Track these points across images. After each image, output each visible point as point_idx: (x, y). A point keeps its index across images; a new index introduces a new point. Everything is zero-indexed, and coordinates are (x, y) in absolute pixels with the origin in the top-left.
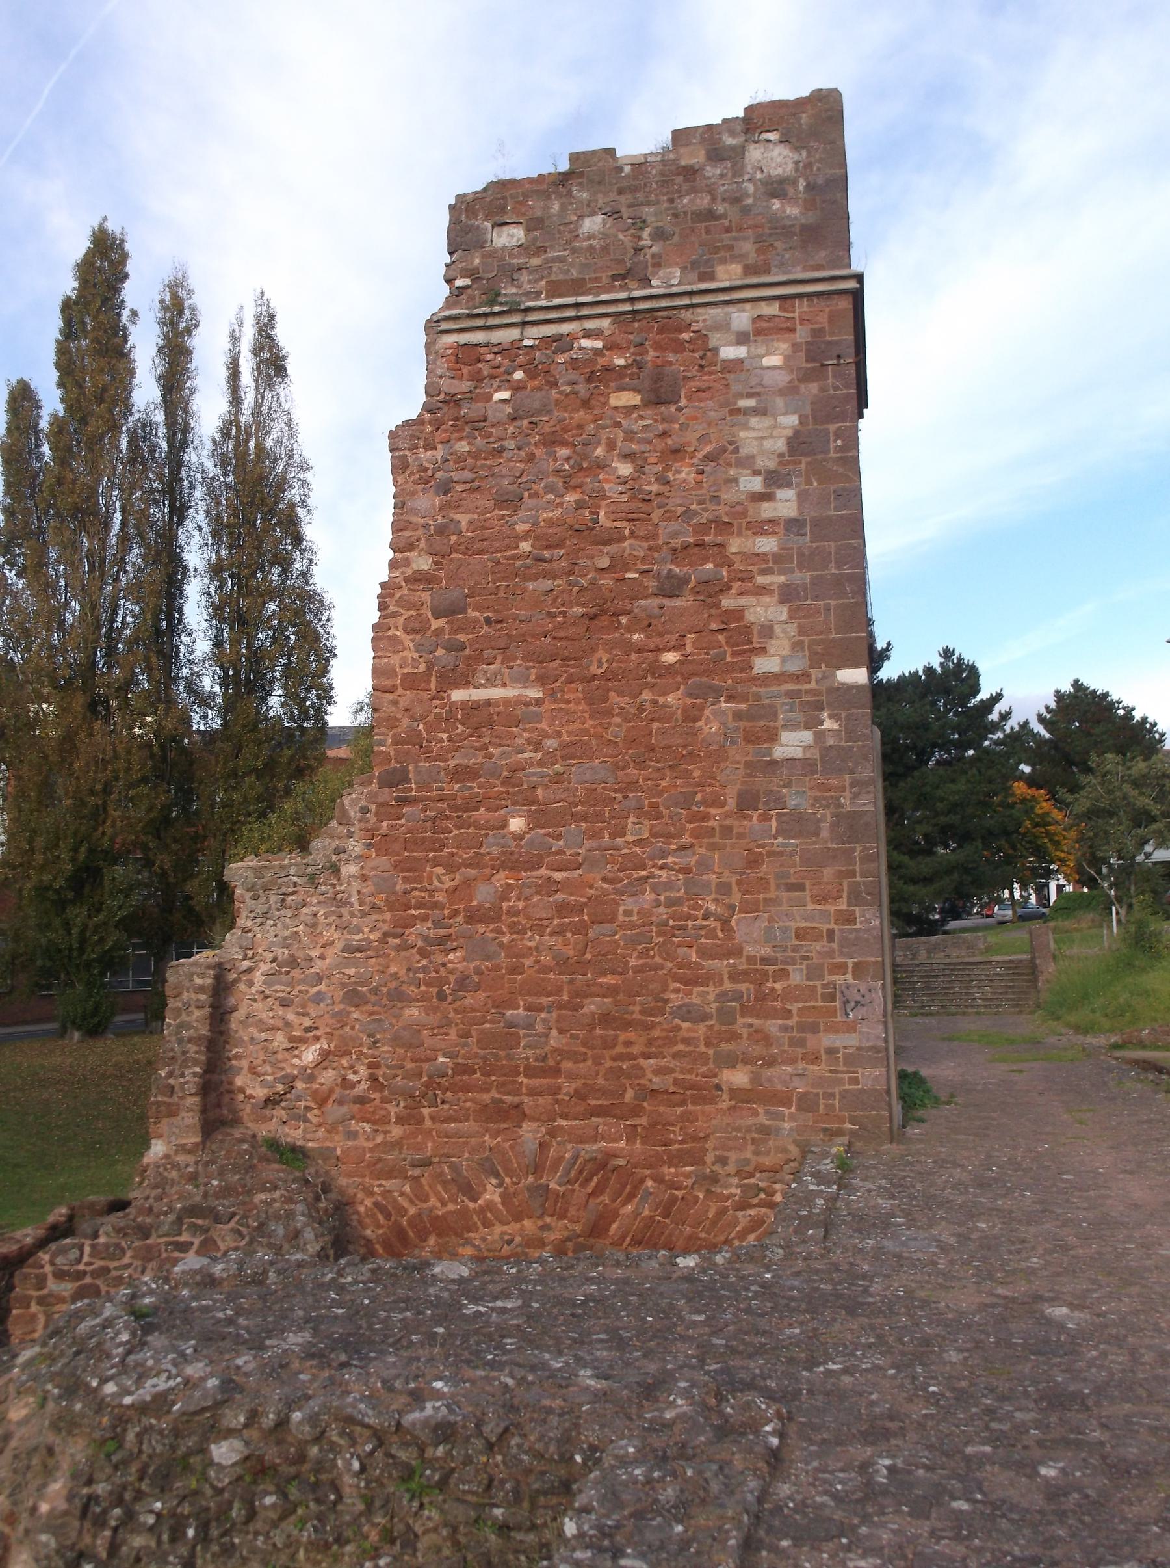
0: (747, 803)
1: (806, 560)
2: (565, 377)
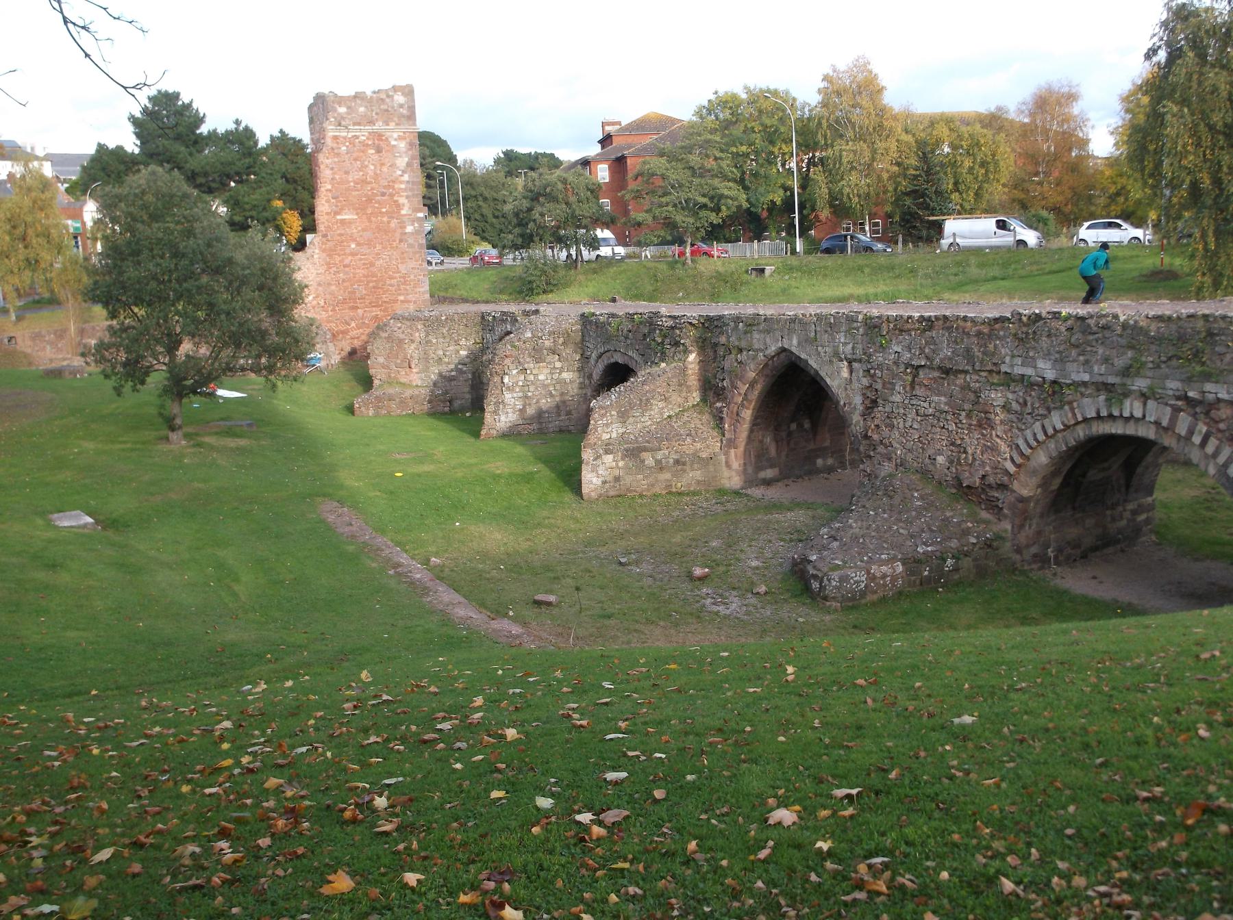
0: (401, 241)
1: (411, 190)
2: (357, 144)
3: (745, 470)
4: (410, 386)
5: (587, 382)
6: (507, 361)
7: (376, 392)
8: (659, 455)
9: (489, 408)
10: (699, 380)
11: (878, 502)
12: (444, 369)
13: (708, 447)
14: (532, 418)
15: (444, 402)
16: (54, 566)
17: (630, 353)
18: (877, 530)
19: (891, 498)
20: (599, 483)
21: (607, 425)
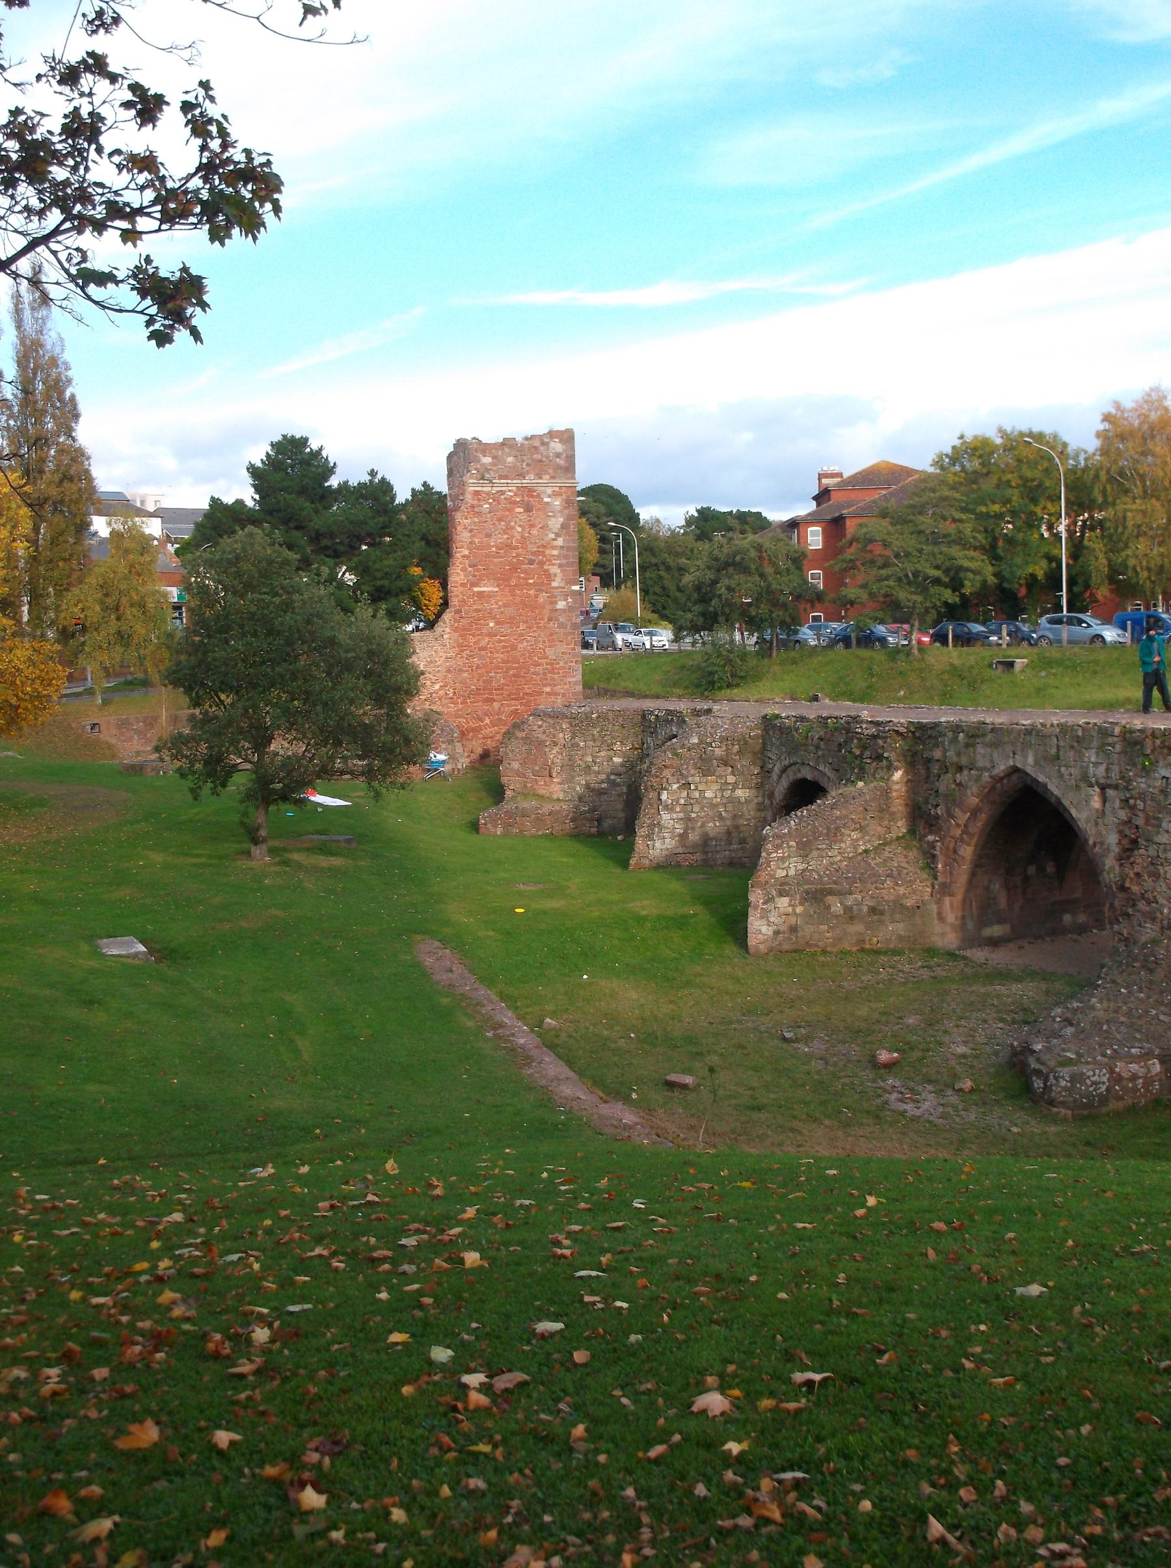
0: (550, 619)
1: (566, 557)
3: (963, 926)
4: (550, 799)
5: (767, 801)
6: (667, 773)
7: (507, 806)
8: (850, 901)
9: (641, 832)
10: (906, 805)
11: (1133, 977)
12: (592, 778)
13: (914, 892)
14: (695, 846)
15: (591, 820)
16: (91, 1002)
17: (821, 768)
18: (1129, 1014)
19: (1151, 971)
20: (770, 933)
21: (783, 859)
